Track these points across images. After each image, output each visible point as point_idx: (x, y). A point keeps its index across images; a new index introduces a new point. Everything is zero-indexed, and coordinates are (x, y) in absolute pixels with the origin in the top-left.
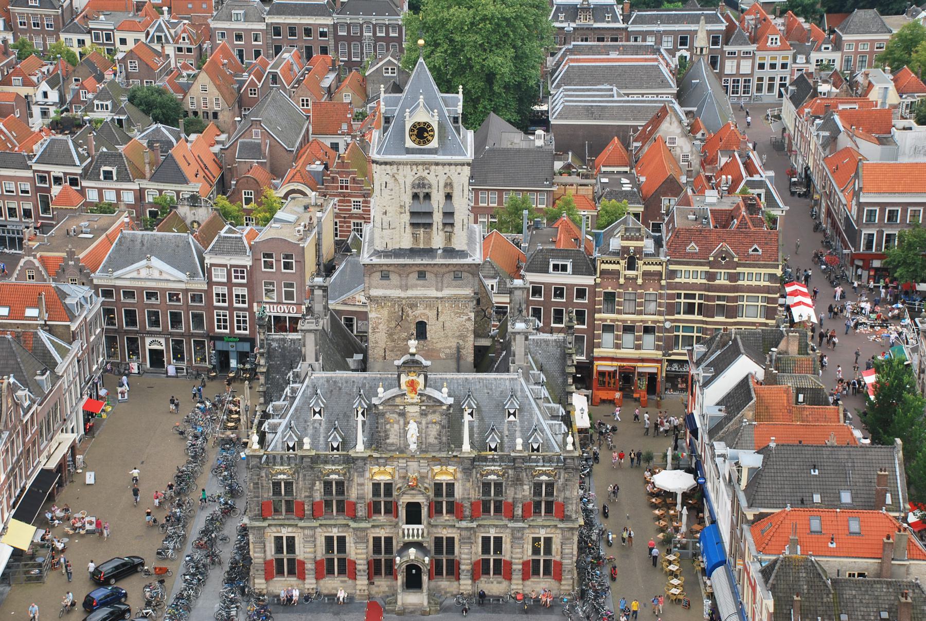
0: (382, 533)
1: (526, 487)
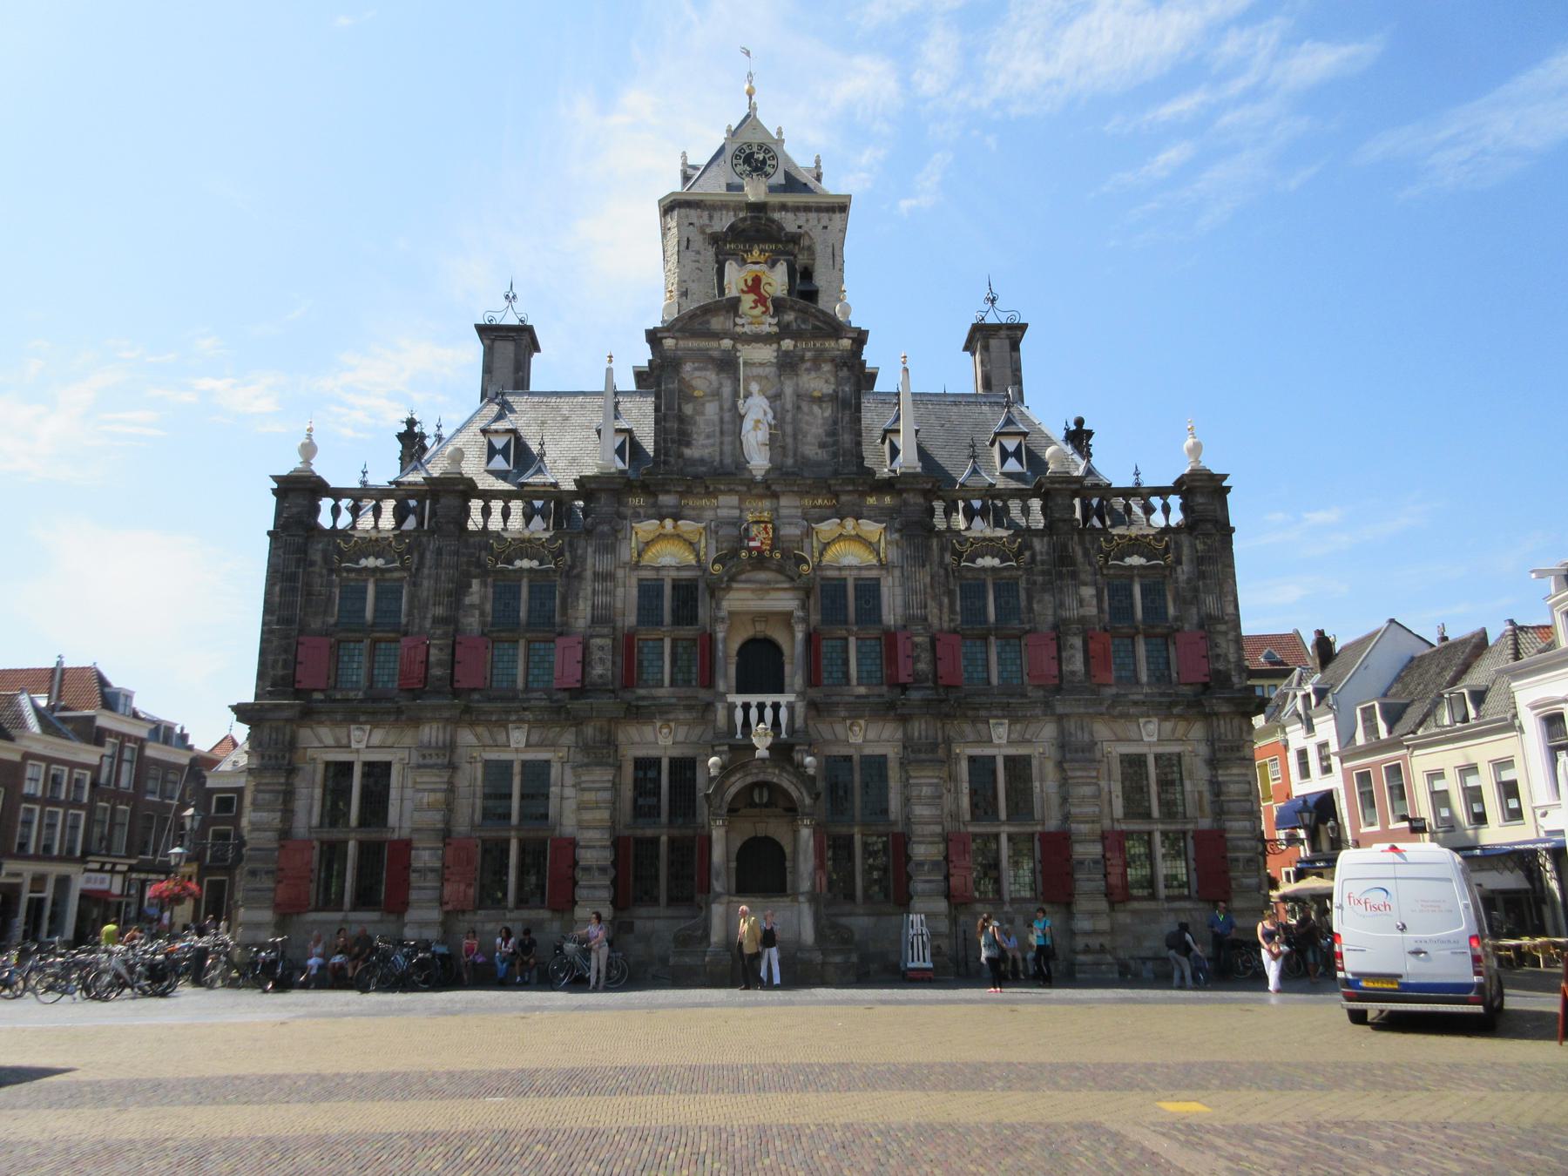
0: (660, 740)
1: (1088, 592)
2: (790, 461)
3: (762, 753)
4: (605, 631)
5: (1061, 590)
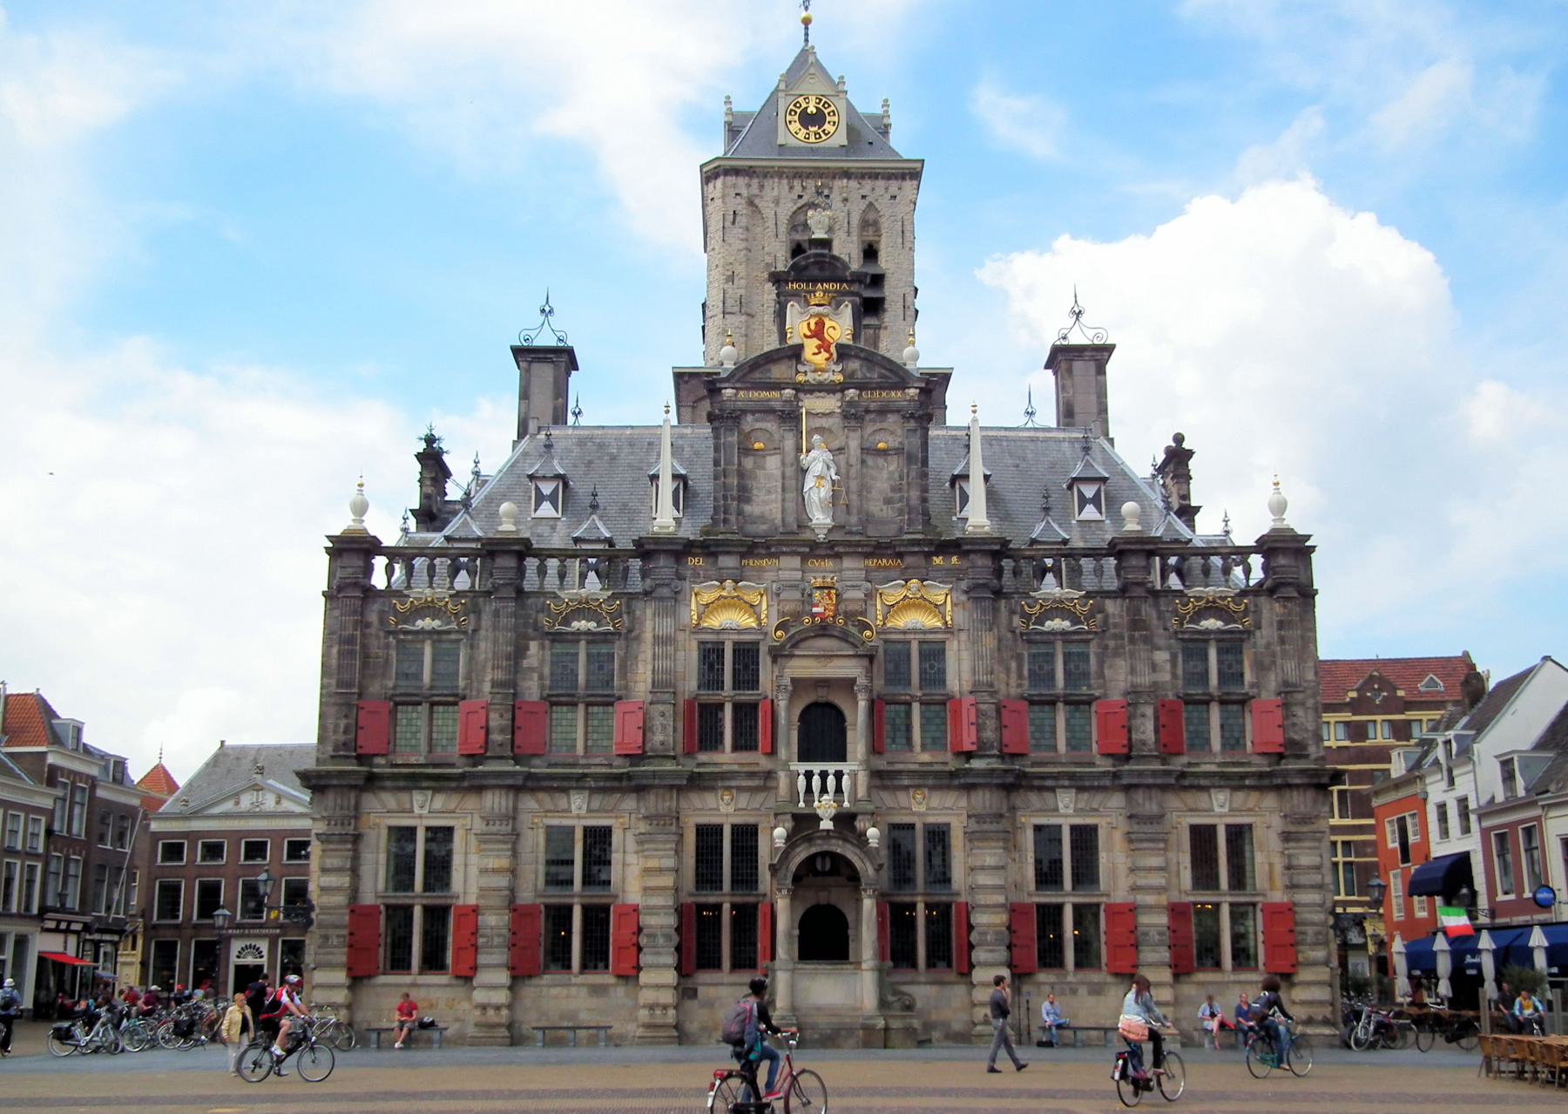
0: (724, 809)
1: (1162, 657)
2: (854, 519)
3: (826, 825)
4: (667, 696)
5: (1132, 655)
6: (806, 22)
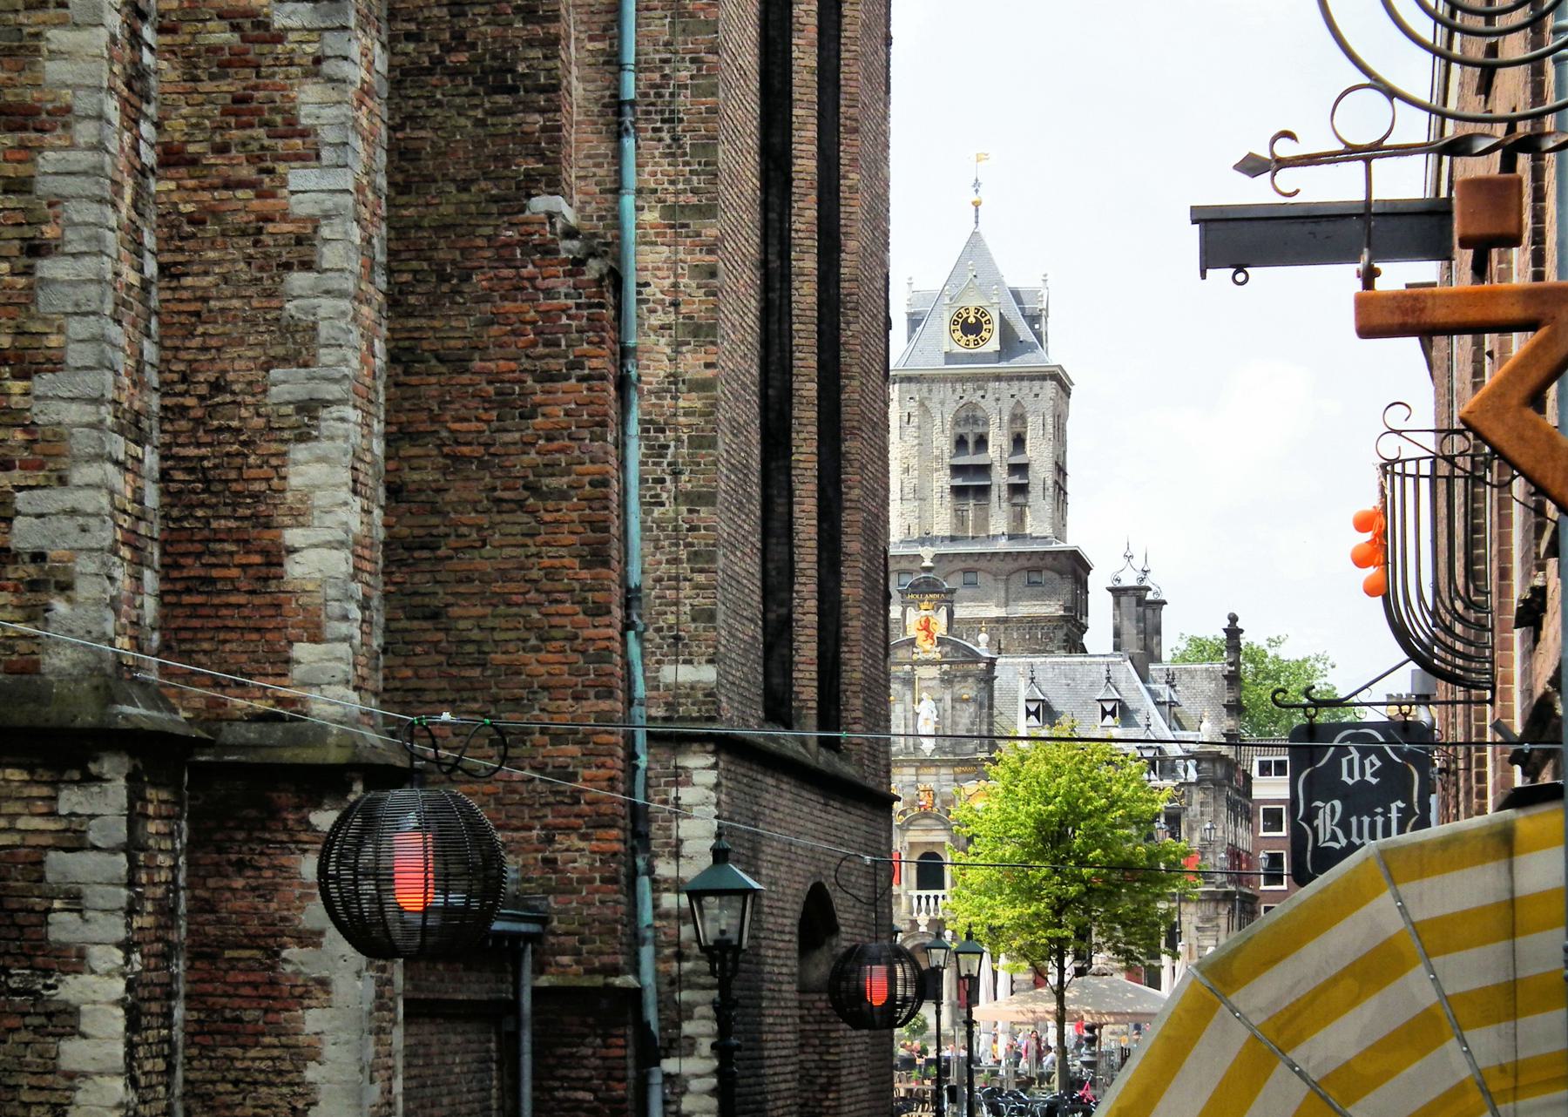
6: (977, 205)
